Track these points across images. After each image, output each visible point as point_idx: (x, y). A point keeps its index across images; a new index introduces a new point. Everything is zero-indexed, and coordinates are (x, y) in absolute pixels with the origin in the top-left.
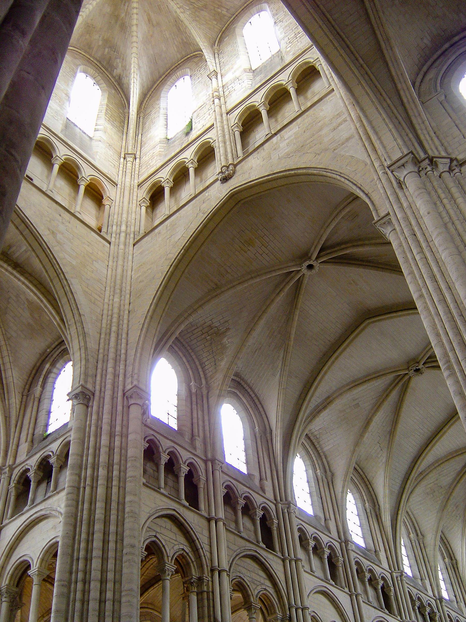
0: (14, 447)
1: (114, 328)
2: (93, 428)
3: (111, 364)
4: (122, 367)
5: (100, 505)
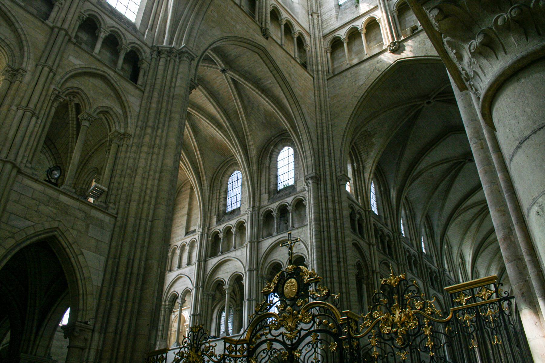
0: (258, 195)
1: (325, 136)
2: (323, 198)
3: (327, 159)
4: (333, 161)
5: (333, 242)
